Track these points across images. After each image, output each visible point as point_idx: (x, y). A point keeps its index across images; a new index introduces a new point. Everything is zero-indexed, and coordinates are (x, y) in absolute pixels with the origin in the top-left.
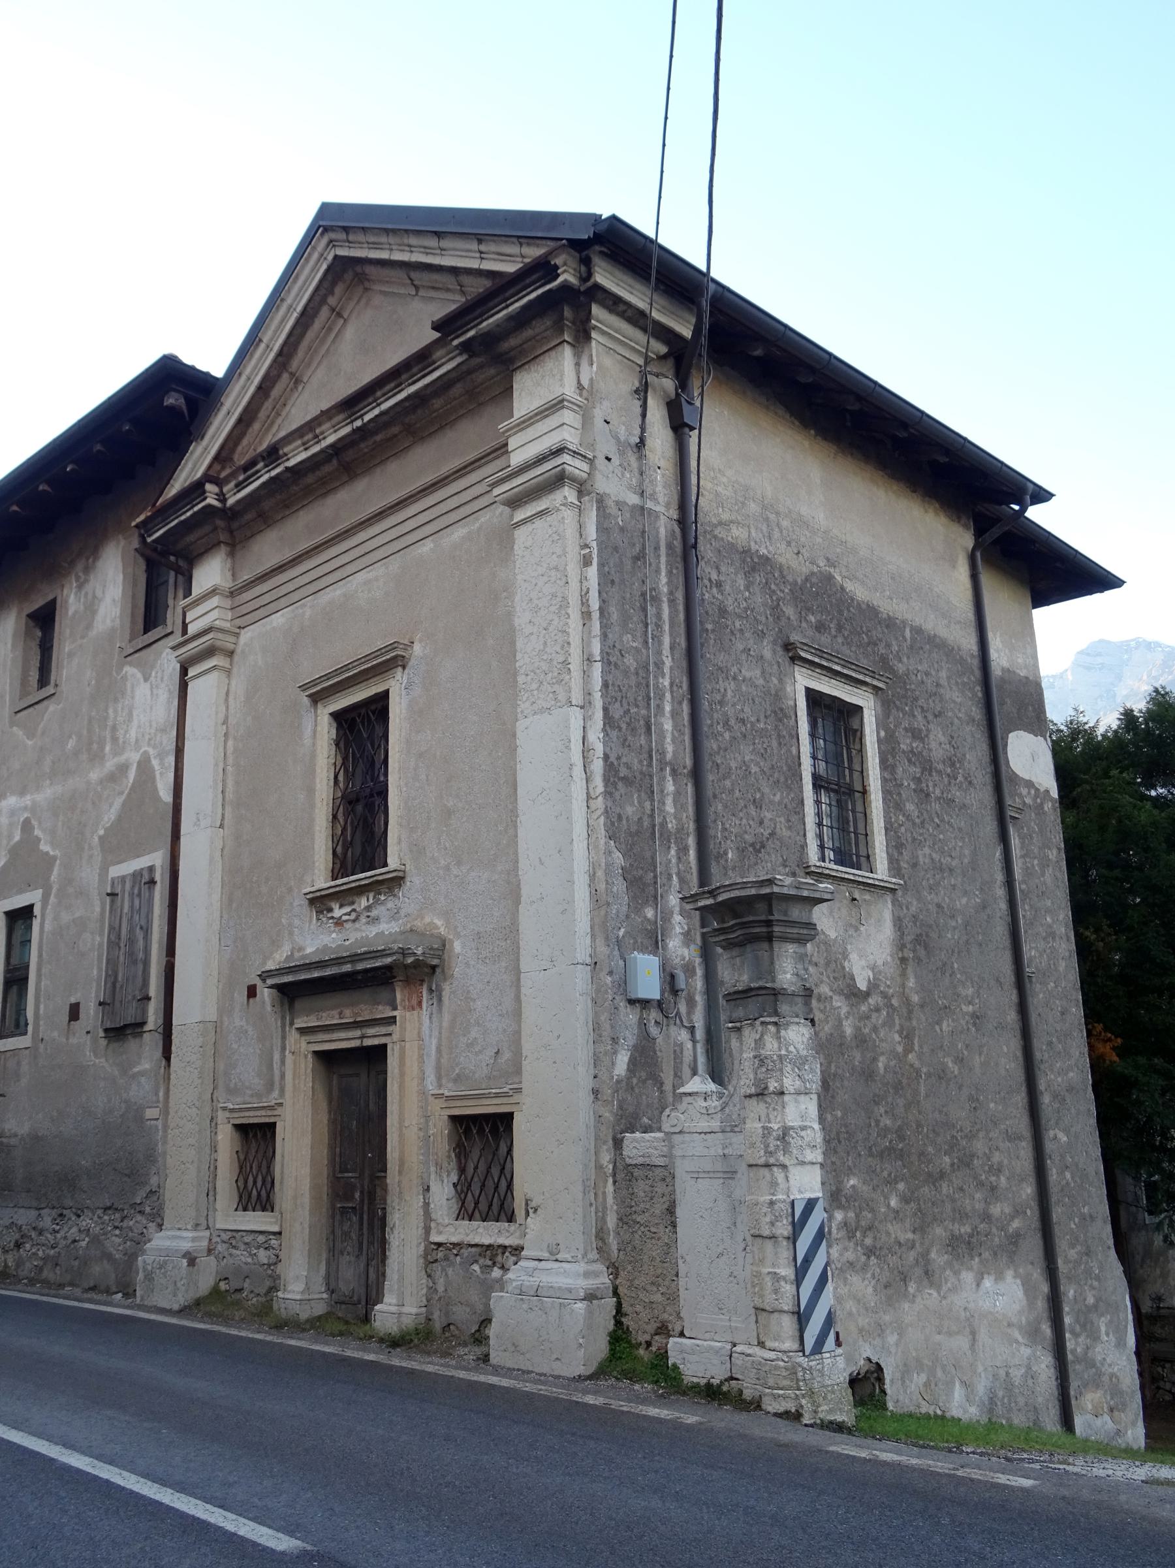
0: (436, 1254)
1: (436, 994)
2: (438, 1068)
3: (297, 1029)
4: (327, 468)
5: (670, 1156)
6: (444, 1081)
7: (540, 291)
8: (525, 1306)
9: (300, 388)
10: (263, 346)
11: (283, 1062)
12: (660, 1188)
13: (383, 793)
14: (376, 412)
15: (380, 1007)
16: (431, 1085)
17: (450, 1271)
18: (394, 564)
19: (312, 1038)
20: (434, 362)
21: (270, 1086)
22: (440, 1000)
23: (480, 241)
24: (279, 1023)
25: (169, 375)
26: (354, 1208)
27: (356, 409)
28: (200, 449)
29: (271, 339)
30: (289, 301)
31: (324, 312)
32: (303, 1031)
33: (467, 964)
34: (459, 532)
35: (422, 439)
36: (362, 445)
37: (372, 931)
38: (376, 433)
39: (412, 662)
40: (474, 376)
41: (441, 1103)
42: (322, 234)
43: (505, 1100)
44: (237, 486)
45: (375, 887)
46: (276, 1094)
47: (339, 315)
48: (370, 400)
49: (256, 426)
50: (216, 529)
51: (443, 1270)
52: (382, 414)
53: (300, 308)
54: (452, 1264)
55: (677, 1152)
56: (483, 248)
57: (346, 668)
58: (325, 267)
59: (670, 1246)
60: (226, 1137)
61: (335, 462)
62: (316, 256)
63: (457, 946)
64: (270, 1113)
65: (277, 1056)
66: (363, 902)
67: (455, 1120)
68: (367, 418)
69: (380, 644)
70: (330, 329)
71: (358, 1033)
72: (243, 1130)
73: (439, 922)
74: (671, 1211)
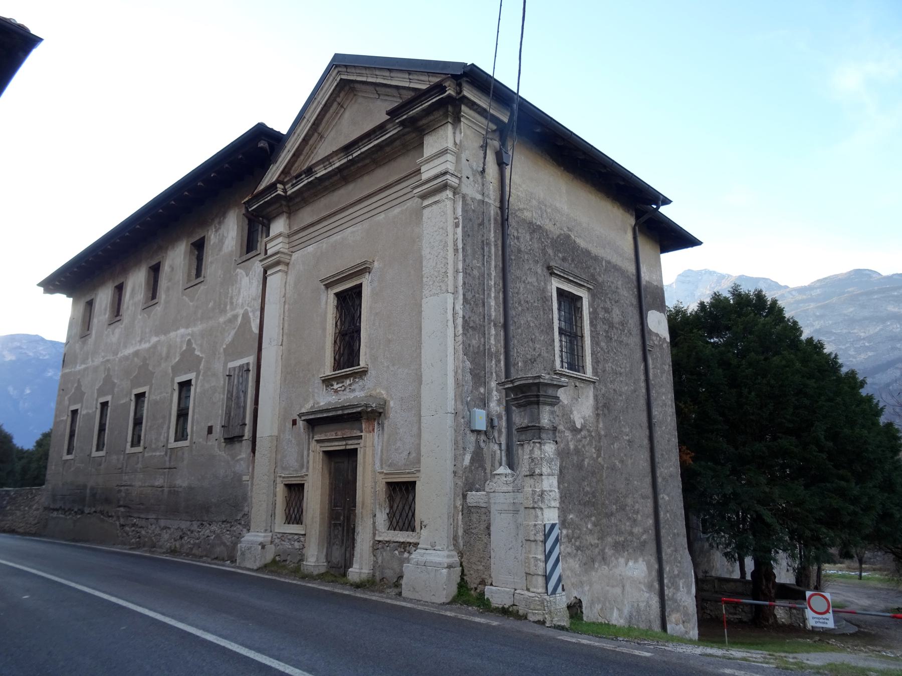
0: (378, 546)
1: (381, 425)
2: (381, 460)
4: (335, 178)
5: (488, 502)
11: (308, 455)
12: (483, 517)
13: (358, 331)
14: (359, 152)
16: (378, 469)
18: (366, 224)
21: (302, 466)
22: (383, 428)
23: (410, 74)
25: (261, 132)
28: (274, 168)
30: (318, 99)
31: (335, 105)
32: (318, 441)
34: (397, 210)
37: (352, 396)
38: (358, 162)
39: (374, 270)
45: (354, 375)
46: (305, 470)
47: (342, 107)
49: (302, 158)
50: (281, 205)
52: (362, 153)
53: (323, 103)
54: (385, 551)
55: (492, 501)
56: (411, 77)
57: (342, 272)
59: (487, 545)
60: (280, 489)
62: (331, 78)
63: (392, 404)
65: (305, 453)
66: (348, 382)
67: (389, 484)
68: (354, 155)
69: (359, 262)
70: (337, 113)
71: (344, 443)
72: (289, 486)
73: (383, 392)
74: (488, 528)
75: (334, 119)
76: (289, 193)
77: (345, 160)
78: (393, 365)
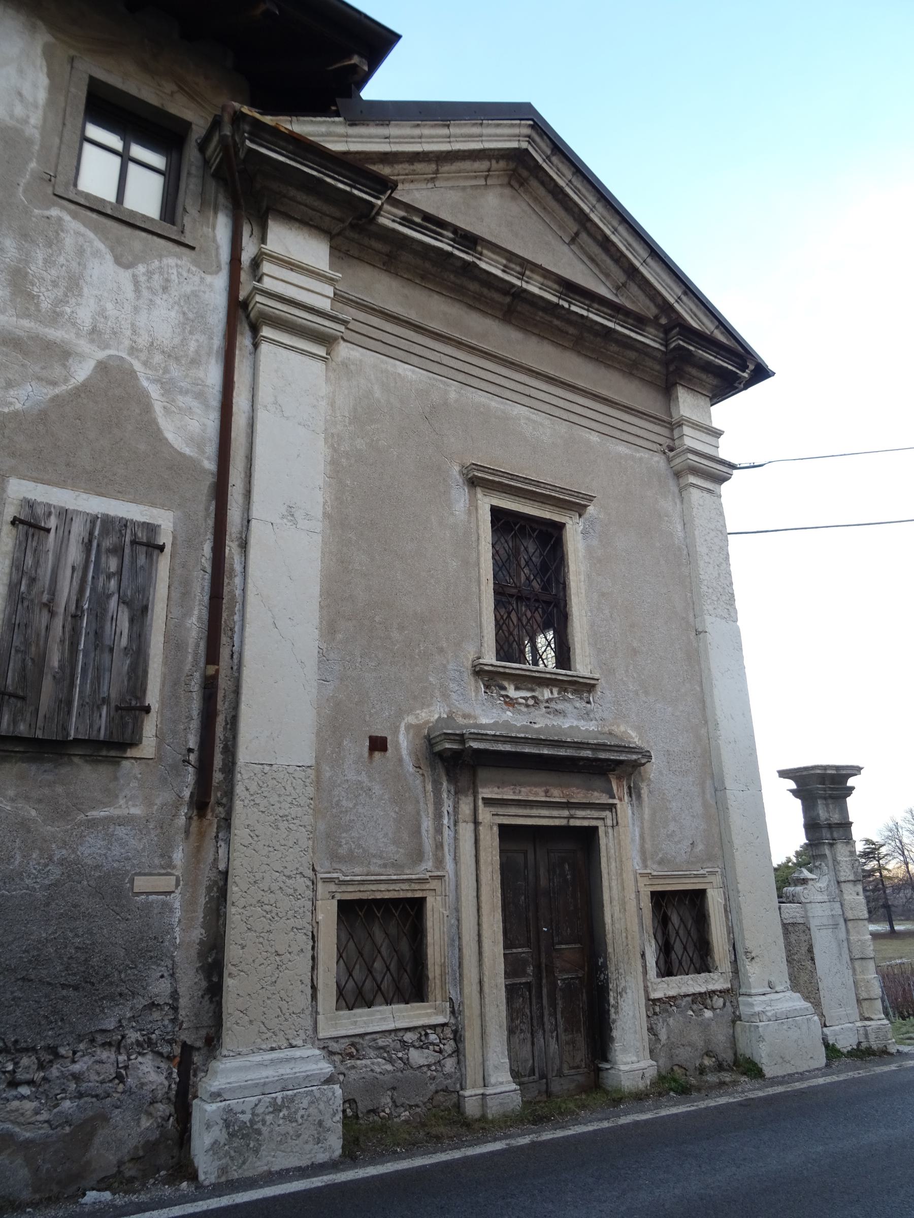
0: (657, 1007)
2: (643, 852)
3: (483, 799)
4: (497, 296)
5: (806, 917)
6: (649, 863)
7: (734, 369)
8: (785, 1027)
9: (430, 185)
10: (445, 131)
11: (439, 830)
12: (803, 937)
14: (585, 313)
15: (596, 794)
17: (671, 1021)
18: (563, 428)
19: (501, 811)
20: (644, 331)
21: (418, 856)
22: (639, 796)
23: (685, 293)
24: (429, 787)
26: (528, 985)
27: (571, 295)
28: (341, 130)
29: (455, 136)
30: (486, 131)
32: (488, 802)
33: (661, 773)
34: (622, 449)
35: (579, 353)
36: (540, 313)
37: (566, 723)
40: (647, 359)
41: (646, 881)
42: (530, 126)
43: (701, 880)
44: (403, 218)
46: (429, 864)
47: (486, 178)
48: (587, 302)
50: (341, 220)
51: (664, 1021)
54: (670, 1015)
55: (810, 914)
56: (684, 298)
57: (538, 483)
58: (514, 145)
59: (813, 972)
61: (508, 299)
62: (516, 131)
64: (417, 887)
65: (427, 824)
66: (547, 694)
68: (573, 308)
71: (566, 813)
73: (633, 734)
74: (810, 950)
75: (466, 178)
76: (383, 221)
77: (555, 299)
78: (646, 693)
